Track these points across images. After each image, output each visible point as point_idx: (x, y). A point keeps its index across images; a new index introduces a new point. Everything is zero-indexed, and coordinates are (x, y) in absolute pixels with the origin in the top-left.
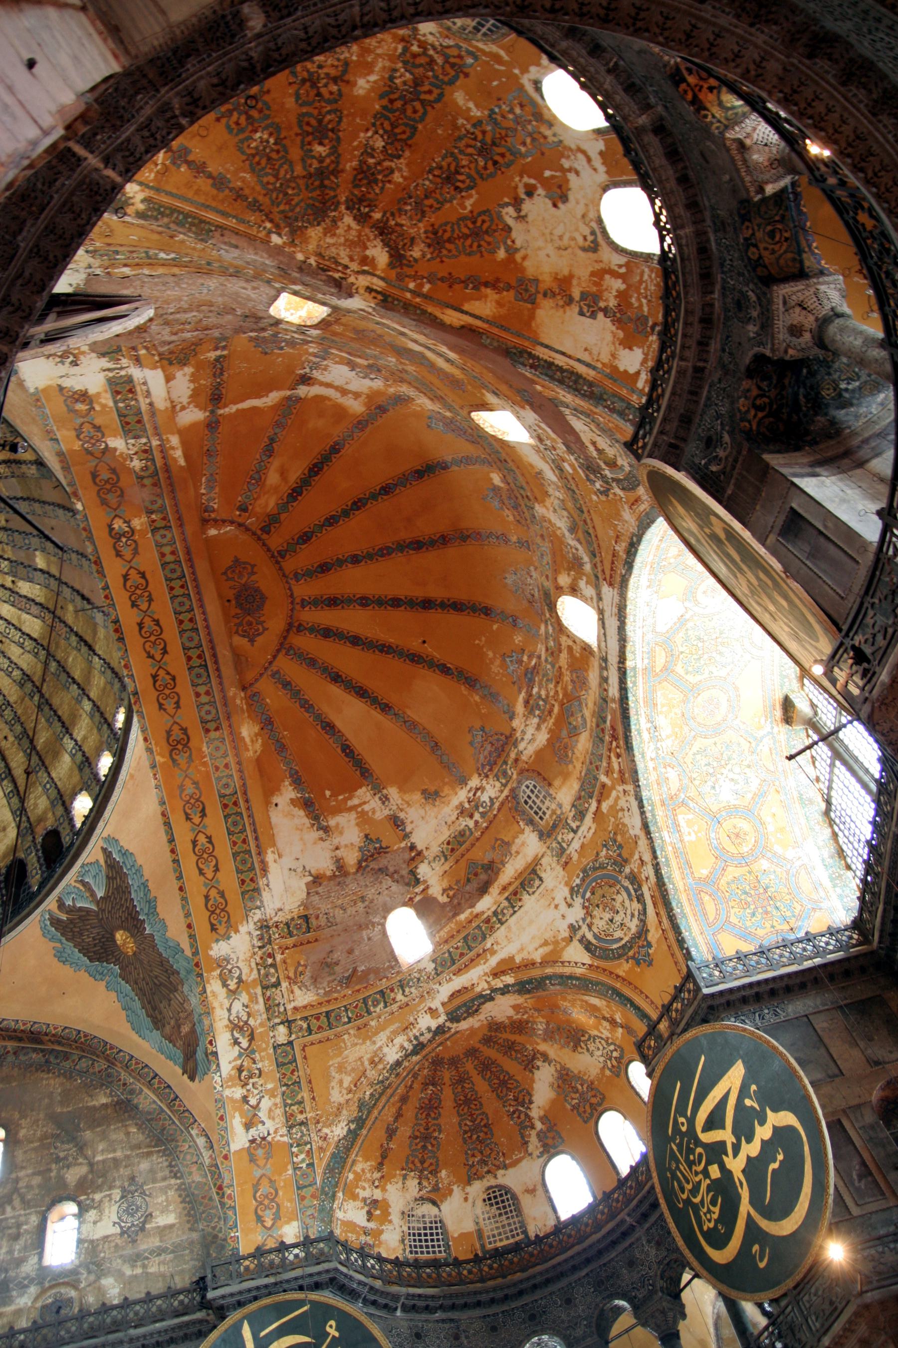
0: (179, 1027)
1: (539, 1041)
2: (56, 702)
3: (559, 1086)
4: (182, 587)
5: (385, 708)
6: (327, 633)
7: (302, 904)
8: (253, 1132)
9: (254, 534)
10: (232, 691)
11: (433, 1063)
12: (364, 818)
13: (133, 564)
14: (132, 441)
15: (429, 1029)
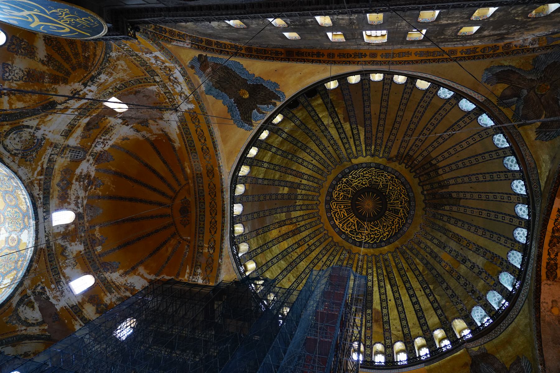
0: (213, 70)
1: (47, 72)
2: (292, 145)
3: (33, 49)
4: (200, 224)
5: (146, 165)
6: (163, 194)
7: (164, 114)
8: (154, 55)
9: (178, 234)
10: (192, 185)
11: (88, 68)
12: (151, 131)
13: (212, 236)
14: (196, 281)
15: (90, 86)
